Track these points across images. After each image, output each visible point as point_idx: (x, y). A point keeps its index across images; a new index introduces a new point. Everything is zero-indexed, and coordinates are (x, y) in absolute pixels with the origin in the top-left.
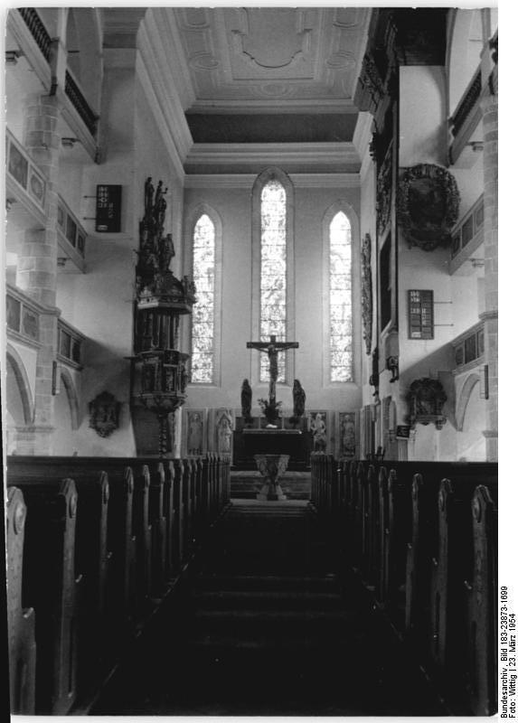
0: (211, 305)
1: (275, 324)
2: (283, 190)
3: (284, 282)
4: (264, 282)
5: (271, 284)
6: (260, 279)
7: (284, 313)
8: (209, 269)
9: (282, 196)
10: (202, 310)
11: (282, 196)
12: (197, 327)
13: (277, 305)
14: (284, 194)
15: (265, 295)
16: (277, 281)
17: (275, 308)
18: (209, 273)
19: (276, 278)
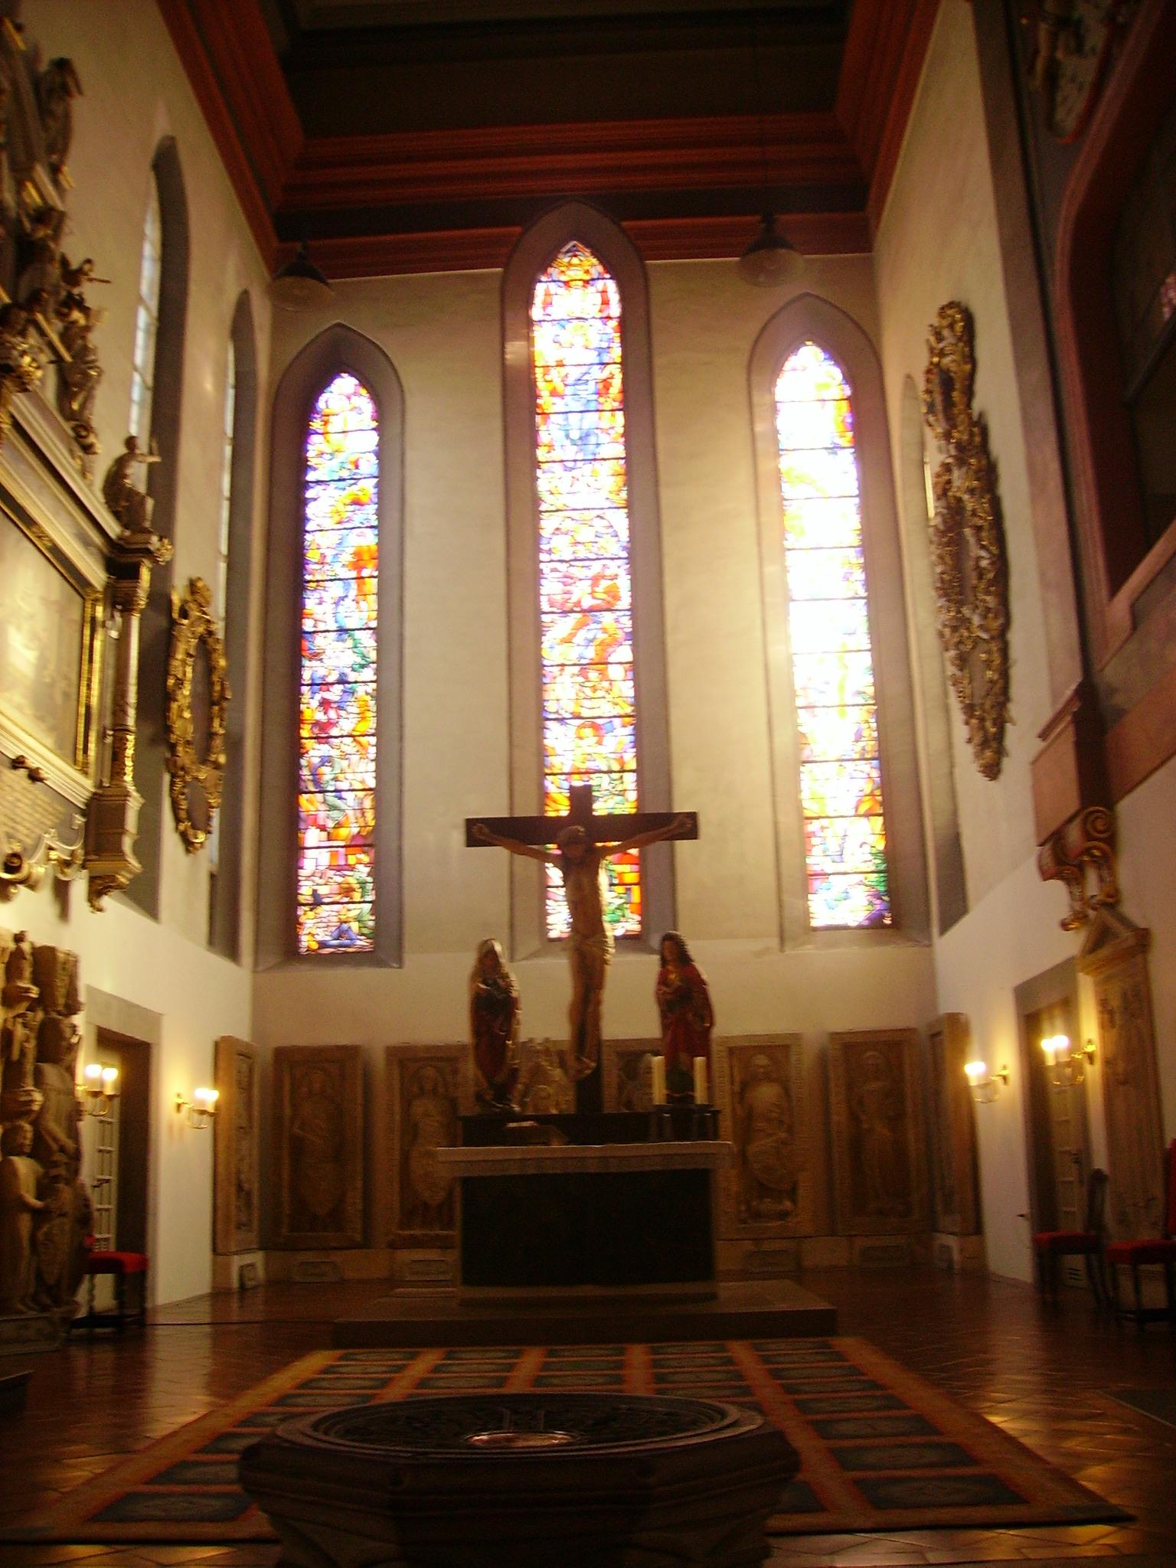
0: (369, 674)
1: (596, 728)
2: (611, 286)
3: (624, 584)
4: (550, 587)
5: (581, 593)
6: (538, 575)
7: (627, 689)
8: (358, 555)
9: (605, 302)
10: (335, 693)
11: (605, 302)
12: (314, 752)
13: (602, 663)
14: (614, 297)
15: (557, 629)
16: (595, 580)
17: (593, 675)
18: (358, 564)
19: (596, 567)
